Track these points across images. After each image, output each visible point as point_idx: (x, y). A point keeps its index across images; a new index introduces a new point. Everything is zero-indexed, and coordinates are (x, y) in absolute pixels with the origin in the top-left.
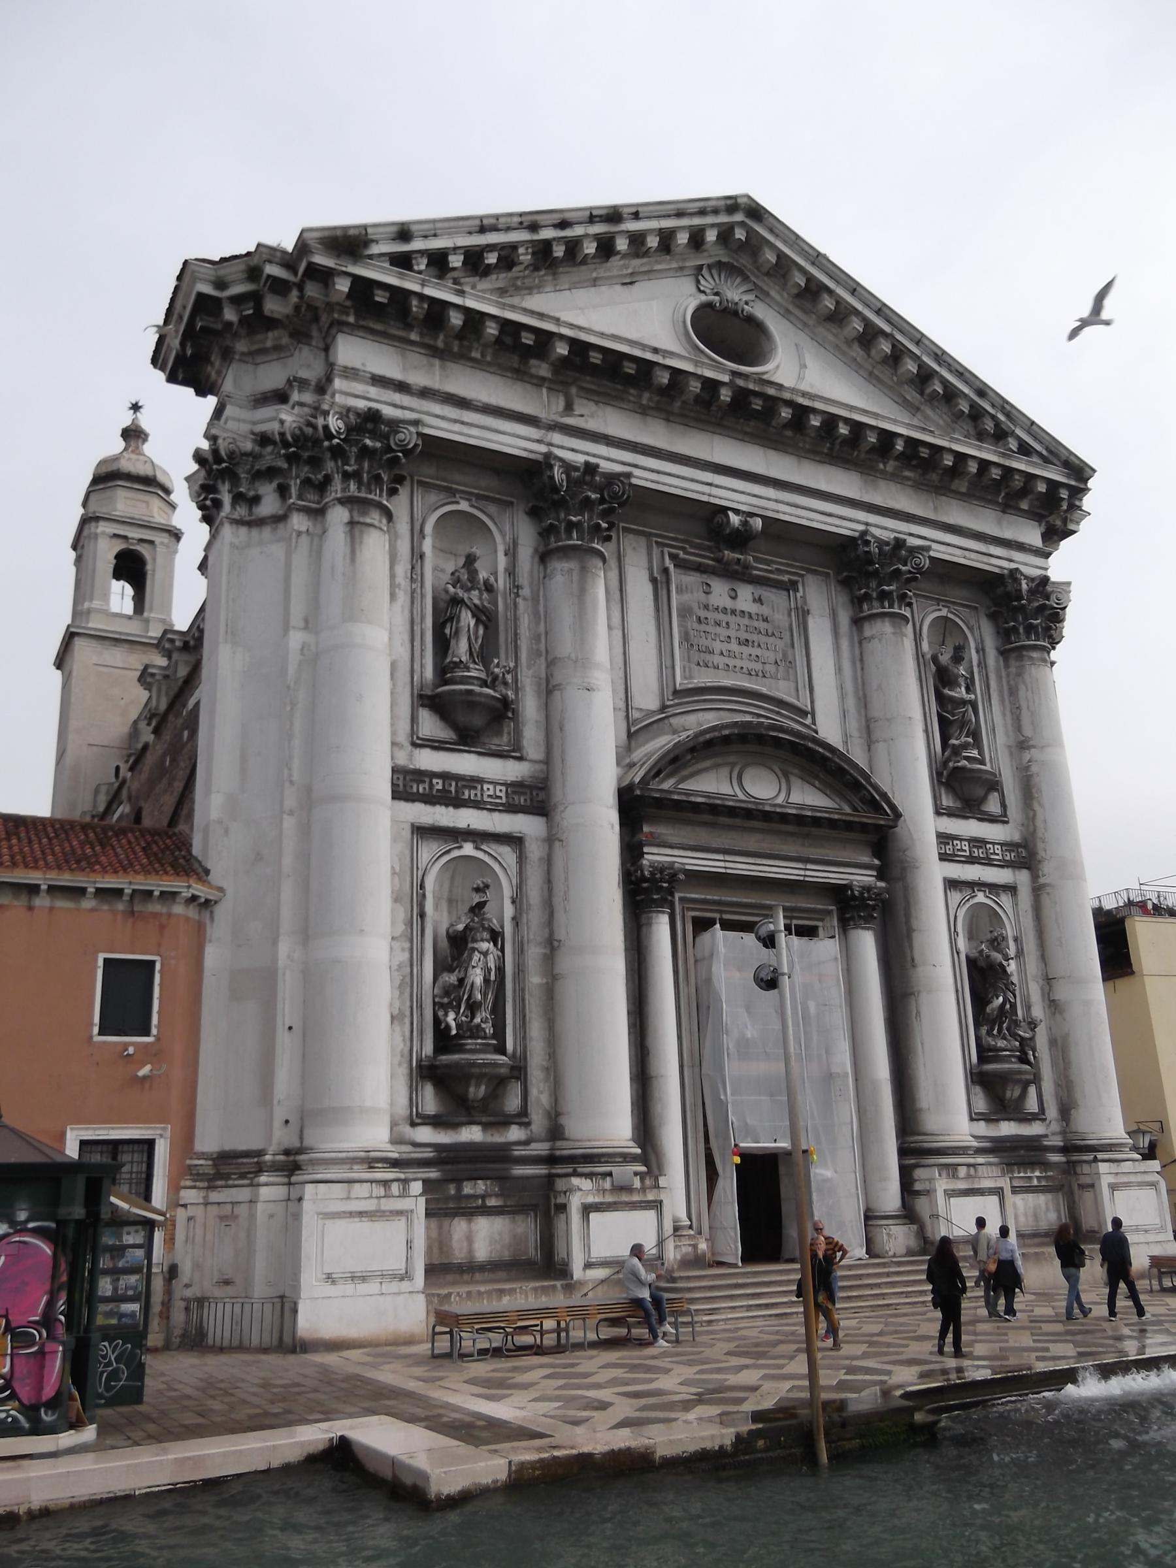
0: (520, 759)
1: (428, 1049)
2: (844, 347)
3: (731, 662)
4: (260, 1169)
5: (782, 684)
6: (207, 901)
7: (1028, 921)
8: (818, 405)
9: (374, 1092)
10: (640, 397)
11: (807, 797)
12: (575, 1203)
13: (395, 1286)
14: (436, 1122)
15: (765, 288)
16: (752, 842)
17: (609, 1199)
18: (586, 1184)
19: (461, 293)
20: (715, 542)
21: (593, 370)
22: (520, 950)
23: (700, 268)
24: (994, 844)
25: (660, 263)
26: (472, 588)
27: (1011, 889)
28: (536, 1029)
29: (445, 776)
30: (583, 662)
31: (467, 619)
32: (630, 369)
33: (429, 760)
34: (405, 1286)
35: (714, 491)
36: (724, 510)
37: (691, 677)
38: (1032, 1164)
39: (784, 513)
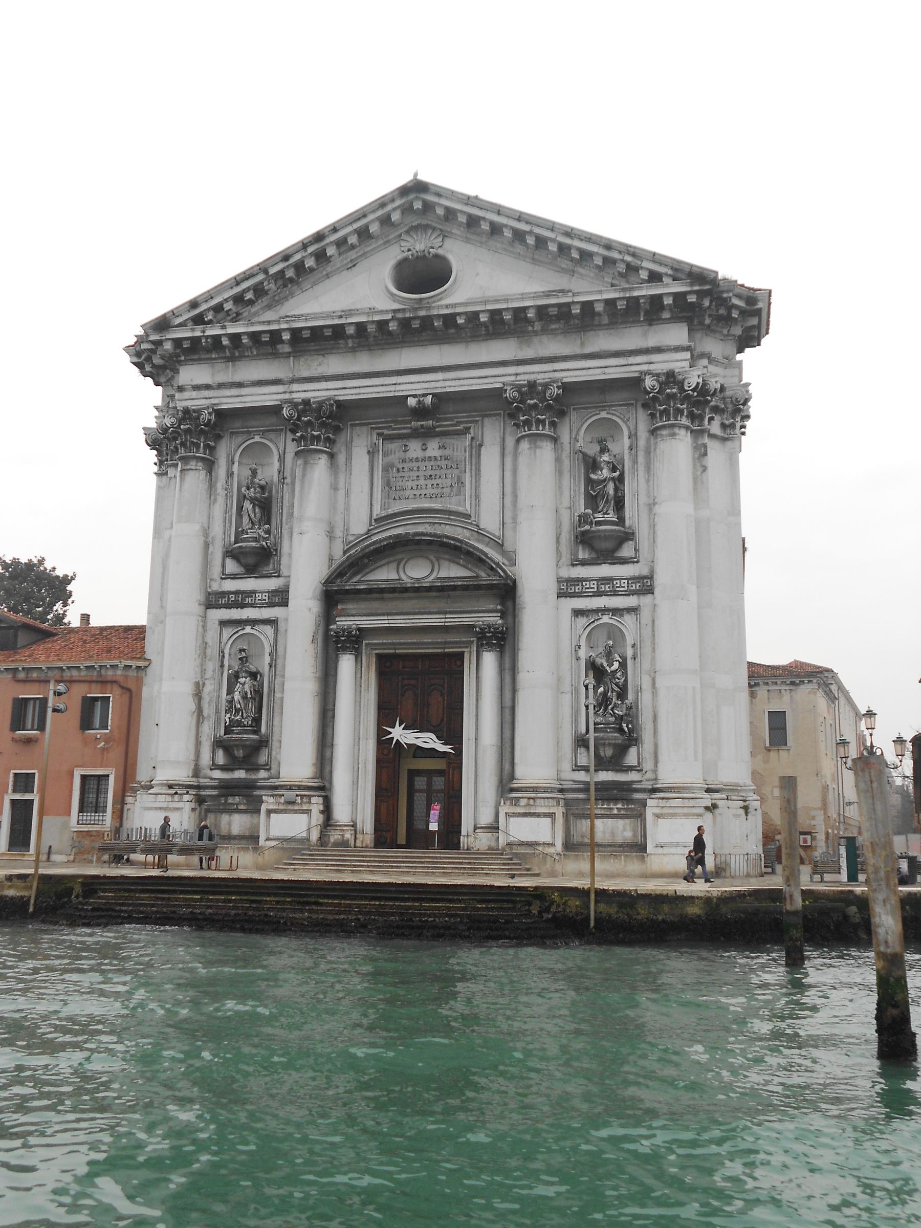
0: (279, 576)
2: (511, 249)
3: (418, 493)
5: (454, 499)
6: (138, 668)
7: (647, 632)
10: (347, 343)
11: (452, 571)
12: (264, 808)
14: (223, 768)
15: (449, 230)
16: (409, 605)
17: (281, 807)
18: (271, 800)
19: (224, 327)
21: (307, 340)
25: (369, 245)
27: (633, 610)
29: (237, 593)
31: (248, 505)
32: (328, 333)
33: (230, 586)
35: (398, 388)
38: (616, 800)
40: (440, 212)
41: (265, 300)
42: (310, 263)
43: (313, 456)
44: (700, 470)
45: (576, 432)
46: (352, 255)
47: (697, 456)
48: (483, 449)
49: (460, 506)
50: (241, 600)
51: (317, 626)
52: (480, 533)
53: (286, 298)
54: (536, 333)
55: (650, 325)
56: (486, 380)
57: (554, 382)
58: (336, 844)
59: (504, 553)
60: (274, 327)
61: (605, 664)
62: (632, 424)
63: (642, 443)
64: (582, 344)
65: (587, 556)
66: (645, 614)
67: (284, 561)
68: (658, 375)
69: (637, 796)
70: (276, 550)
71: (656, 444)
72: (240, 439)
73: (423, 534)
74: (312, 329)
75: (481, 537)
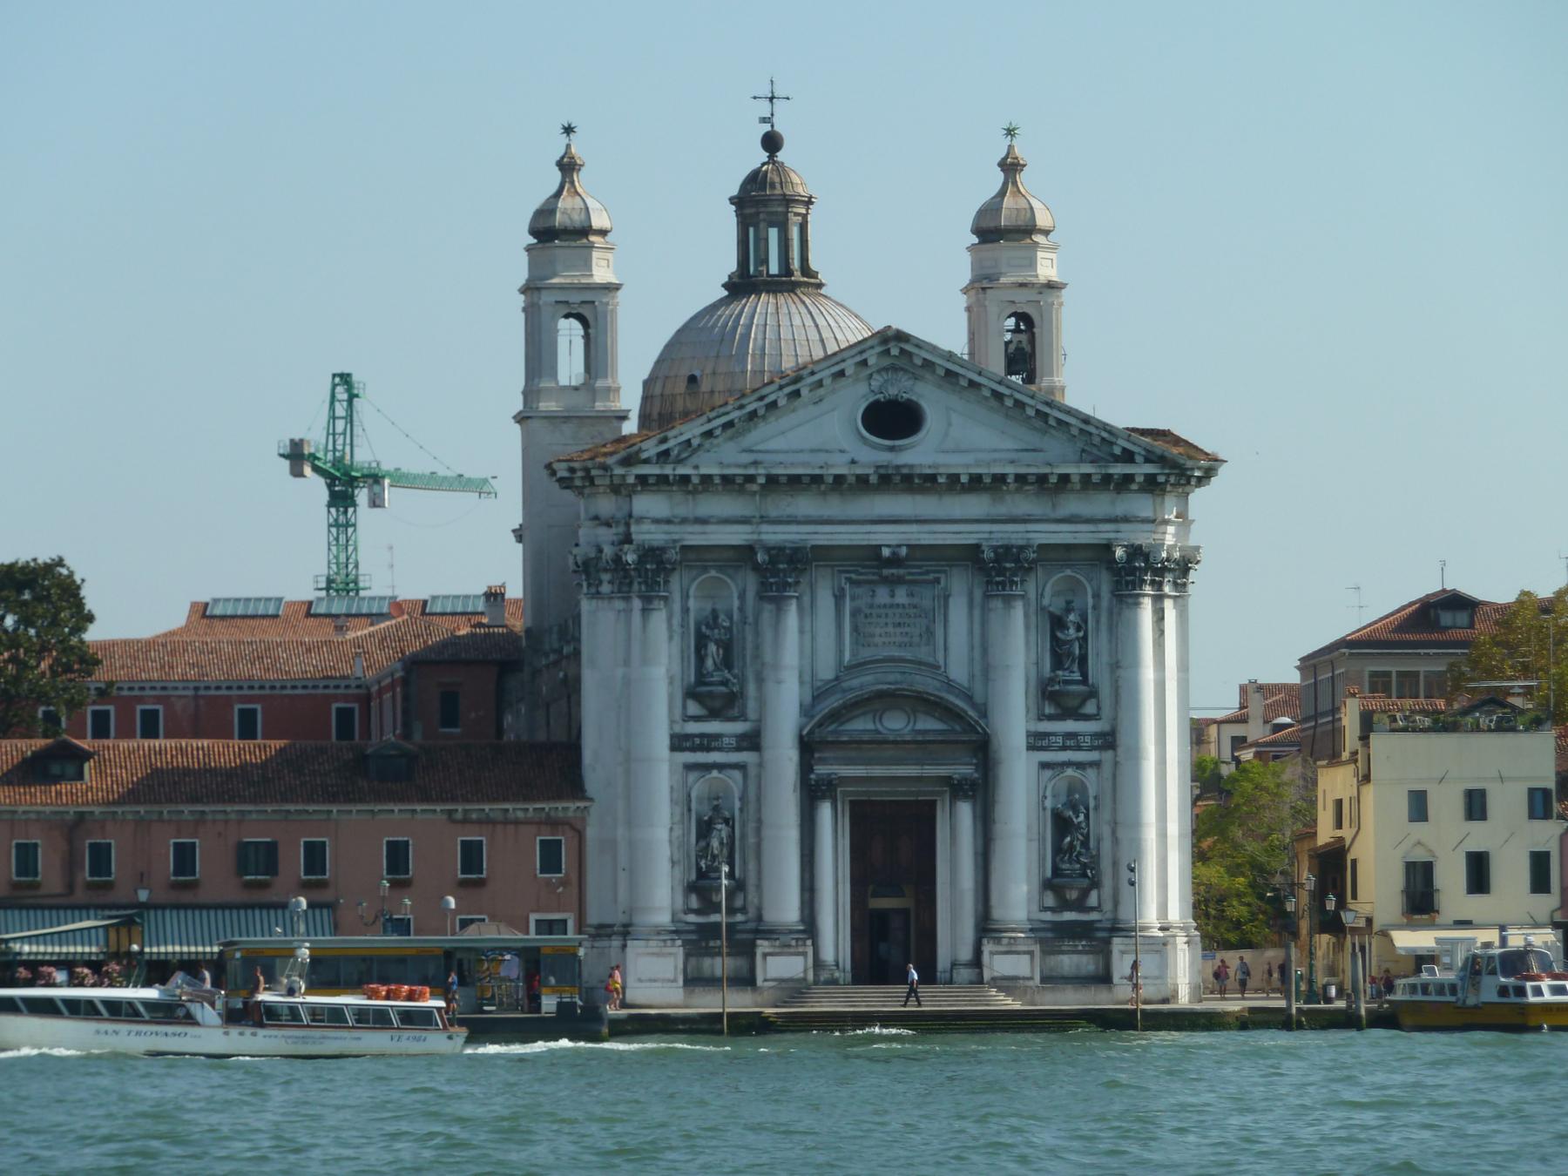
1: (693, 876)
3: (887, 640)
8: (941, 471)
9: (662, 896)
11: (929, 724)
12: (759, 952)
14: (697, 912)
18: (766, 943)
22: (743, 825)
23: (871, 376)
27: (1096, 764)
28: (752, 866)
29: (702, 736)
30: (777, 667)
31: (712, 648)
33: (693, 728)
36: (879, 547)
38: (1080, 938)
40: (918, 362)
41: (730, 432)
42: (782, 402)
45: (1045, 588)
46: (821, 391)
50: (707, 743)
52: (950, 685)
54: (1008, 492)
58: (827, 983)
59: (974, 705)
60: (751, 471)
63: (1105, 603)
64: (1054, 506)
66: (1107, 769)
67: (751, 705)
69: (1100, 934)
72: (695, 572)
74: (789, 477)
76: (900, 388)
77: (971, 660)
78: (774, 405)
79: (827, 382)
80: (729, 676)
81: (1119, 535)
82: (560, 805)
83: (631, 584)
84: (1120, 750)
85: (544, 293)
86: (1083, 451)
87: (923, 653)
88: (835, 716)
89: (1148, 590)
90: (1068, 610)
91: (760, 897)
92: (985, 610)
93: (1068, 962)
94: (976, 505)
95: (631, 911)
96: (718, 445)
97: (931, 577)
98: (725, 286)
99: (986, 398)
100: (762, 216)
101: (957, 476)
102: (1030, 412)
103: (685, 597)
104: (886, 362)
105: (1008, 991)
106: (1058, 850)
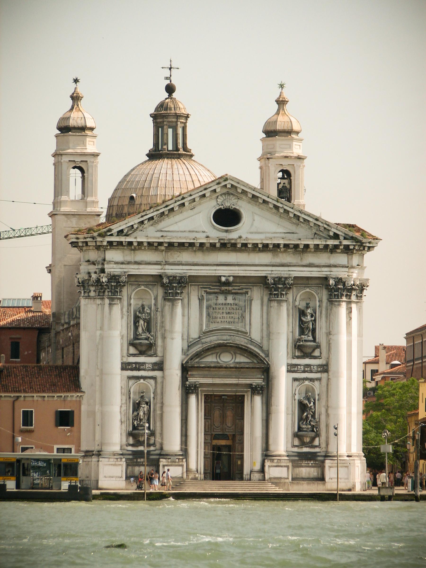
0: (157, 356)
1: (131, 429)
3: (223, 320)
4: (93, 455)
5: (240, 324)
6: (81, 396)
7: (324, 389)
11: (242, 359)
12: (161, 464)
13: (119, 479)
14: (133, 445)
17: (170, 464)
18: (164, 460)
20: (219, 286)
22: (155, 405)
23: (218, 197)
24: (314, 366)
26: (143, 313)
27: (319, 379)
28: (158, 424)
29: (136, 363)
30: (172, 332)
31: (141, 322)
34: (121, 479)
35: (217, 272)
36: (221, 276)
37: (209, 327)
38: (310, 460)
39: (241, 273)
40: (240, 191)
41: (151, 222)
42: (176, 209)
43: (176, 301)
44: (349, 319)
45: (296, 297)
47: (347, 312)
48: (253, 301)
49: (242, 327)
50: (138, 367)
51: (180, 381)
52: (252, 341)
53: (161, 221)
54: (281, 252)
55: (331, 253)
56: (258, 272)
57: (290, 277)
58: (192, 479)
59: (263, 351)
60: (161, 240)
61: (308, 404)
62: (319, 295)
64: (301, 259)
65: (299, 354)
66: (324, 381)
68: (335, 278)
69: (319, 458)
70: (155, 344)
71: (332, 307)
73: (231, 343)
75: (252, 343)
76: (230, 203)
77: (262, 330)
78: (172, 210)
79: (197, 199)
80: (149, 335)
81: (332, 273)
82: (69, 394)
83: (104, 292)
84: (330, 373)
85: (63, 156)
86: (315, 234)
87: (239, 327)
88: (198, 355)
89: (344, 298)
90: (308, 307)
91: (162, 439)
92: (269, 307)
93: (306, 471)
94: (265, 258)
95: (102, 444)
96: (146, 228)
97: (244, 290)
98: (148, 155)
99: (270, 208)
100: (165, 123)
101: (257, 244)
102: (291, 215)
103: (129, 298)
104: (225, 190)
105: (276, 484)
106: (300, 419)
